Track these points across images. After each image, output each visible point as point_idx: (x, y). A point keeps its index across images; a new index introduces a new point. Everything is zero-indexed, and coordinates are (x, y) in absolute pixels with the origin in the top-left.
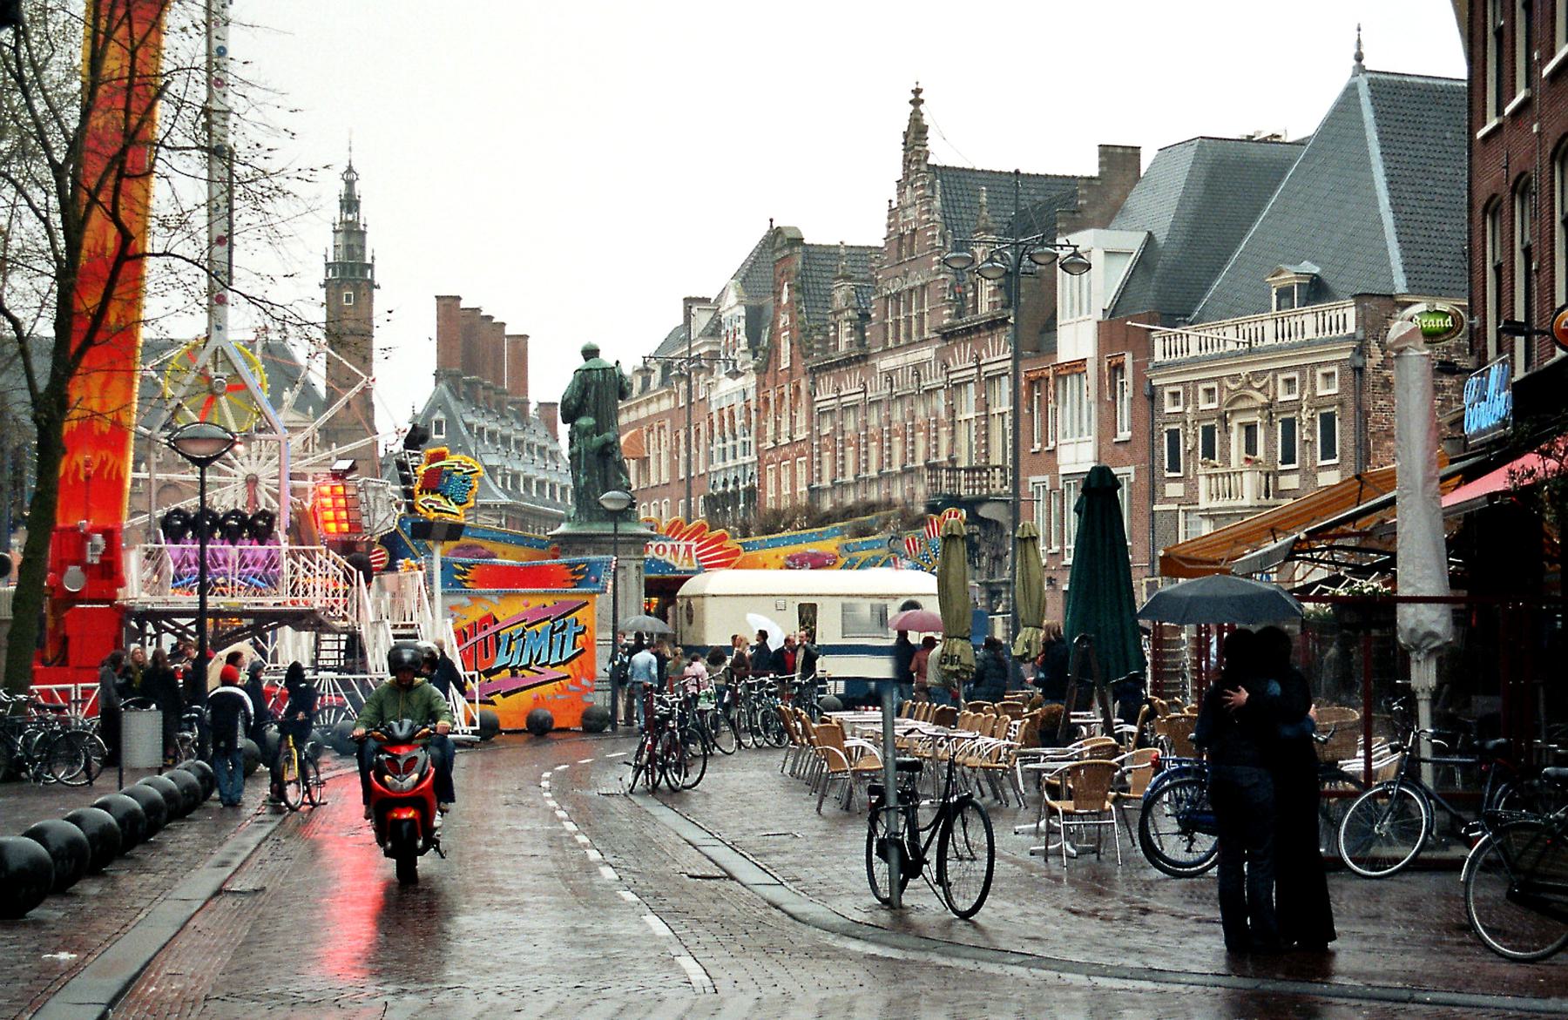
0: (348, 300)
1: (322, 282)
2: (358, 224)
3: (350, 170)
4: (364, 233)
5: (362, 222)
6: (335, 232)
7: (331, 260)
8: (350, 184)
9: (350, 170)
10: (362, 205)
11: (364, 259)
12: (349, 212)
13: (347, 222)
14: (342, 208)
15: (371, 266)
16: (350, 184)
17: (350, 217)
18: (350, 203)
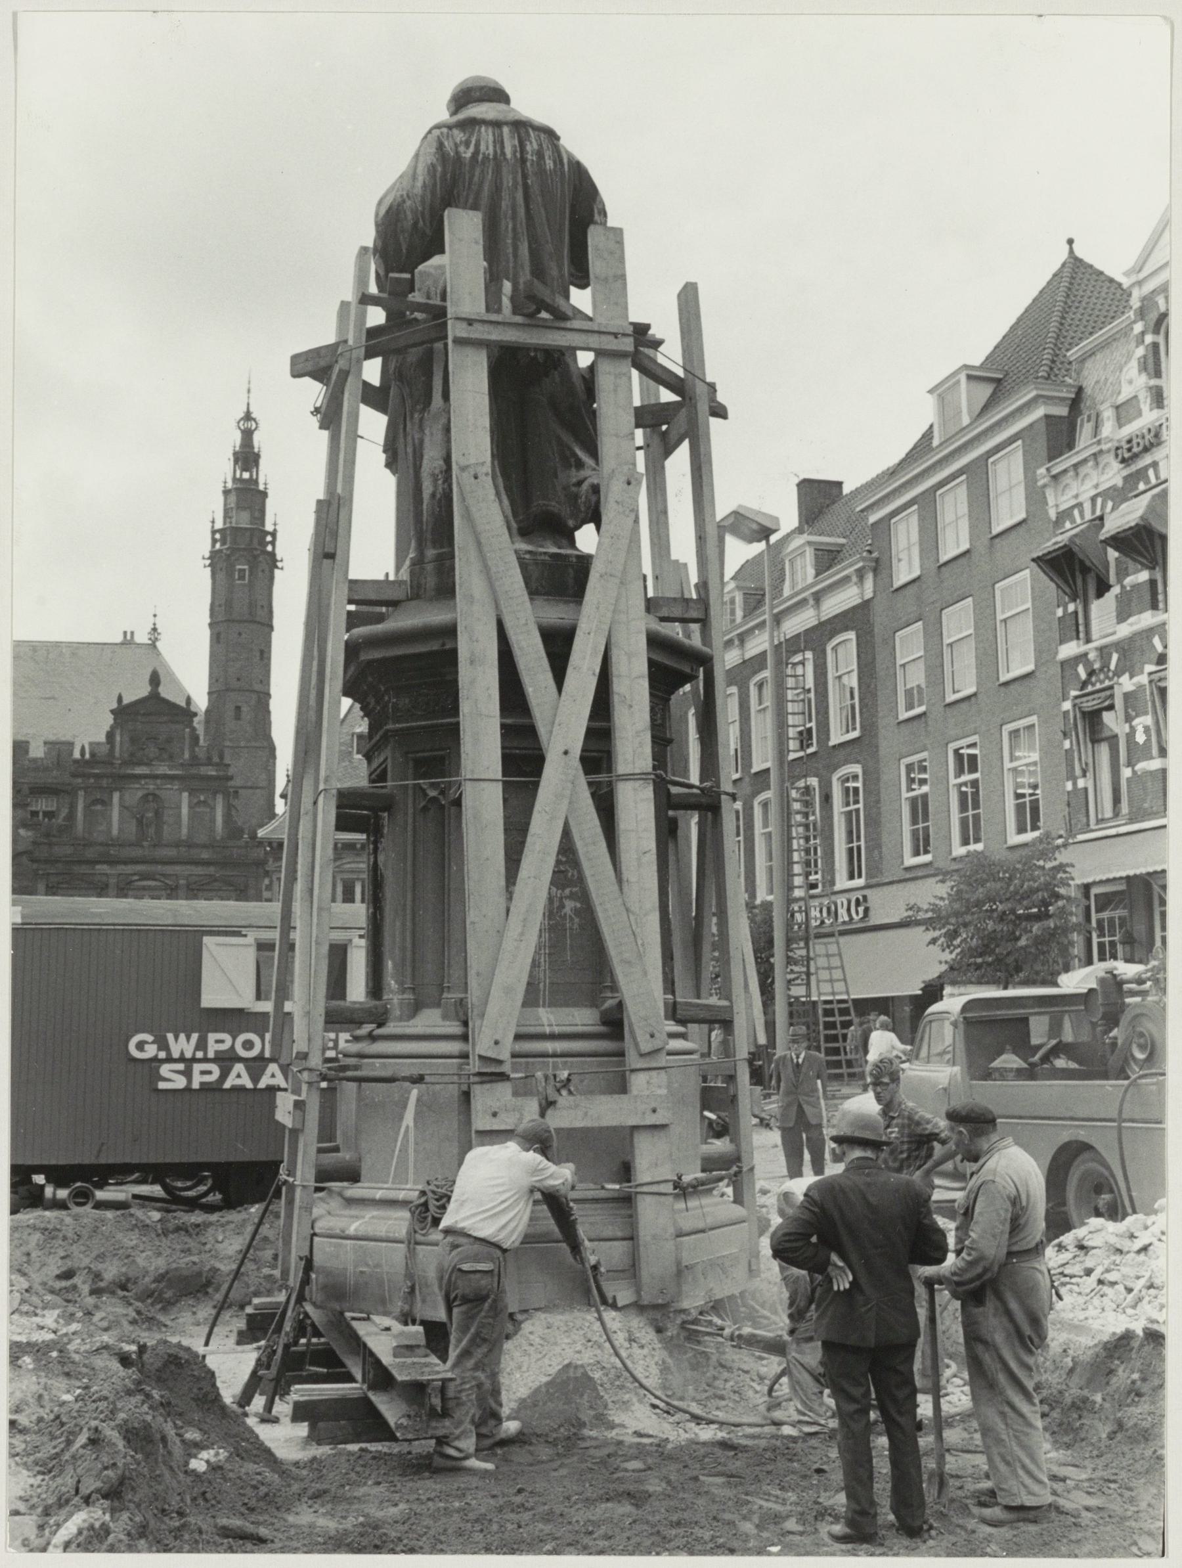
0: (242, 578)
1: (207, 555)
2: (256, 482)
3: (248, 416)
4: (264, 495)
5: (261, 481)
6: (226, 492)
7: (219, 525)
8: (248, 435)
9: (248, 416)
10: (262, 462)
11: (263, 524)
12: (244, 469)
13: (241, 480)
14: (236, 462)
15: (274, 534)
16: (248, 435)
17: (246, 475)
18: (247, 457)
